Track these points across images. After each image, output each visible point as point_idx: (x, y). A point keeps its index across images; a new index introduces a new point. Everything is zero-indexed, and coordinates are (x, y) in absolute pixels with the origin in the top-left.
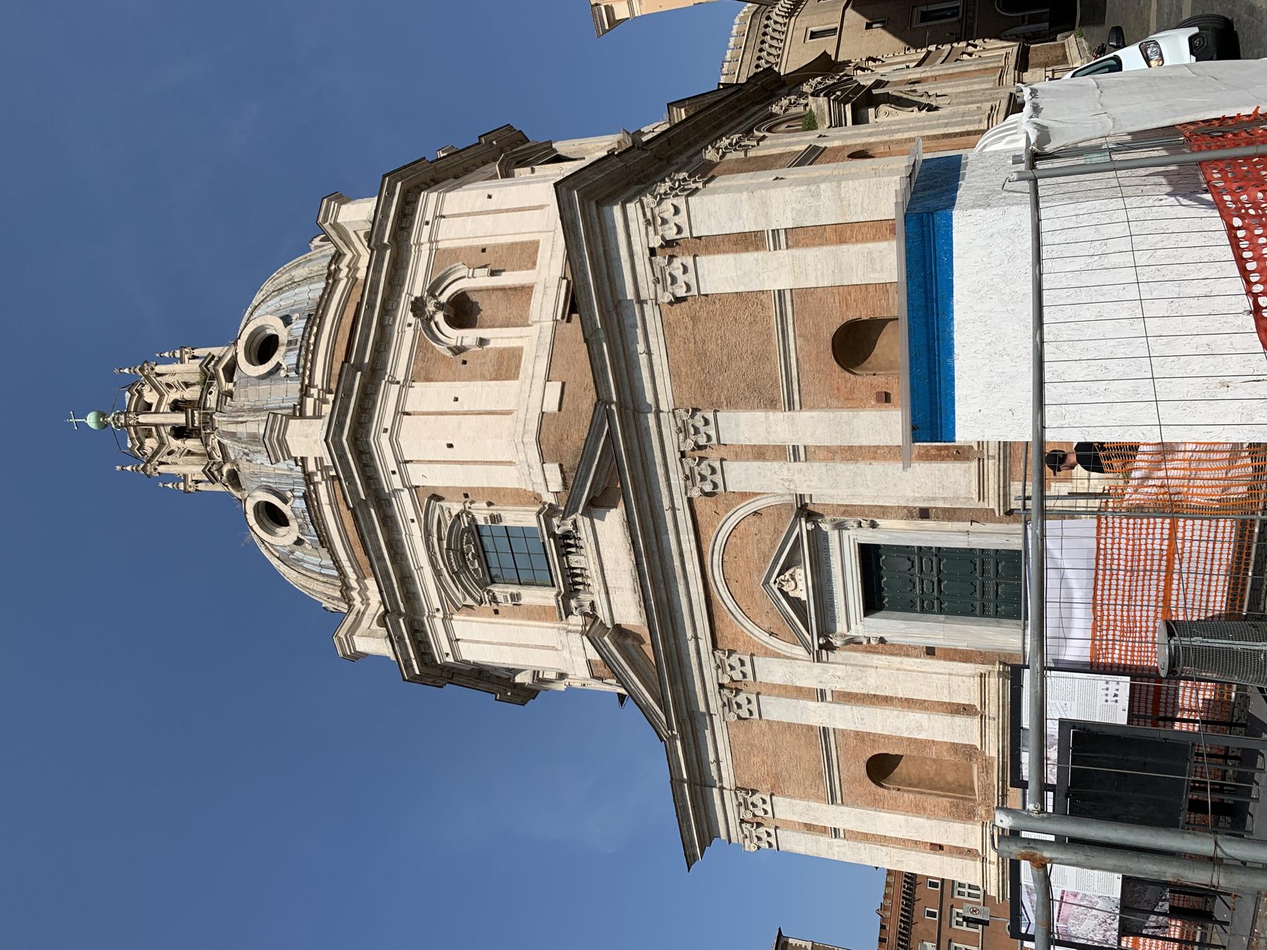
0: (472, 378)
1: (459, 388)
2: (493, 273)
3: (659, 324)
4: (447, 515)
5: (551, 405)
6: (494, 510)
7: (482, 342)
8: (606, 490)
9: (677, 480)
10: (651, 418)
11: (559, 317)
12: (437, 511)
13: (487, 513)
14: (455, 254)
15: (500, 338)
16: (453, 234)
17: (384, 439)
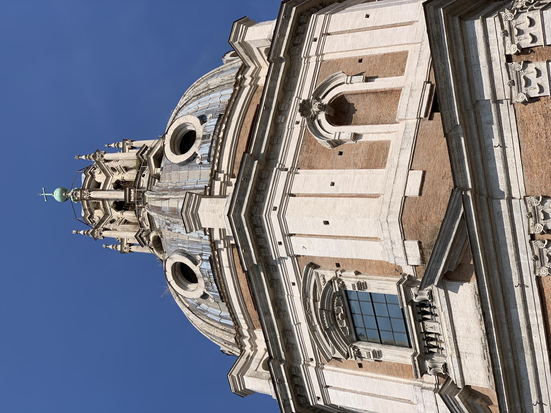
0: (347, 166)
1: (336, 175)
2: (368, 79)
3: (513, 121)
4: (322, 281)
5: (413, 191)
6: (361, 278)
7: (356, 136)
8: (460, 265)
9: (526, 260)
10: (504, 204)
11: (422, 116)
12: (314, 277)
13: (355, 281)
14: (336, 64)
15: (371, 133)
16: (336, 48)
17: (274, 215)
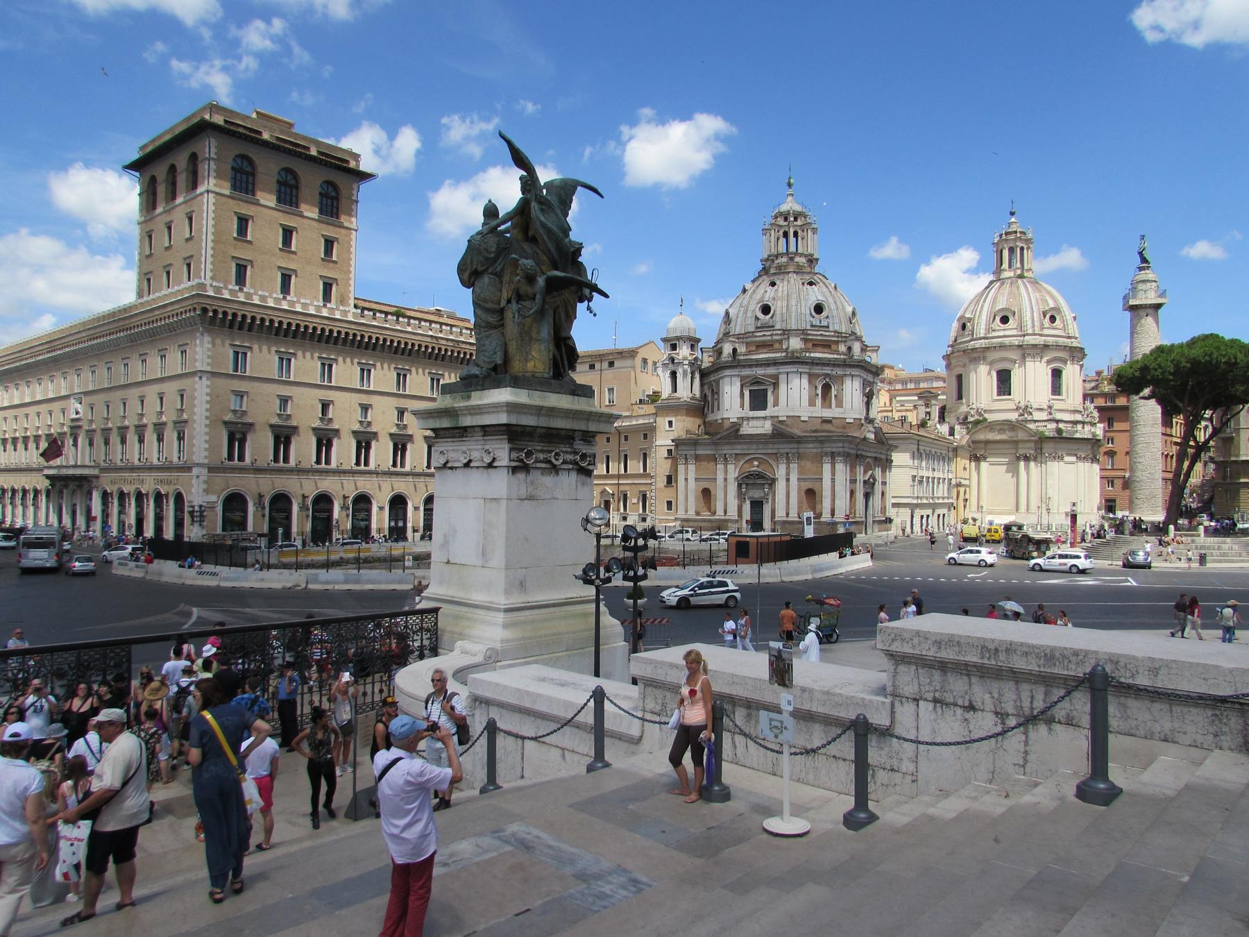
15: (819, 401)
